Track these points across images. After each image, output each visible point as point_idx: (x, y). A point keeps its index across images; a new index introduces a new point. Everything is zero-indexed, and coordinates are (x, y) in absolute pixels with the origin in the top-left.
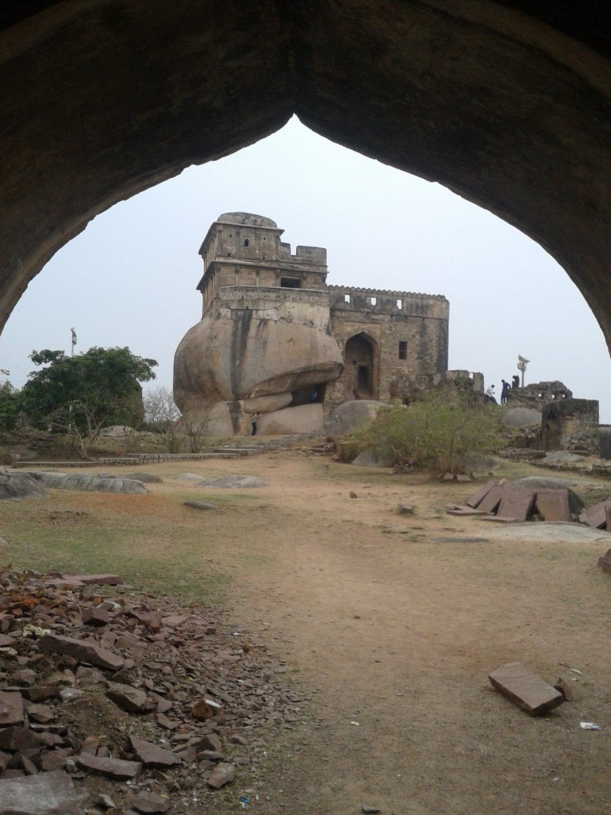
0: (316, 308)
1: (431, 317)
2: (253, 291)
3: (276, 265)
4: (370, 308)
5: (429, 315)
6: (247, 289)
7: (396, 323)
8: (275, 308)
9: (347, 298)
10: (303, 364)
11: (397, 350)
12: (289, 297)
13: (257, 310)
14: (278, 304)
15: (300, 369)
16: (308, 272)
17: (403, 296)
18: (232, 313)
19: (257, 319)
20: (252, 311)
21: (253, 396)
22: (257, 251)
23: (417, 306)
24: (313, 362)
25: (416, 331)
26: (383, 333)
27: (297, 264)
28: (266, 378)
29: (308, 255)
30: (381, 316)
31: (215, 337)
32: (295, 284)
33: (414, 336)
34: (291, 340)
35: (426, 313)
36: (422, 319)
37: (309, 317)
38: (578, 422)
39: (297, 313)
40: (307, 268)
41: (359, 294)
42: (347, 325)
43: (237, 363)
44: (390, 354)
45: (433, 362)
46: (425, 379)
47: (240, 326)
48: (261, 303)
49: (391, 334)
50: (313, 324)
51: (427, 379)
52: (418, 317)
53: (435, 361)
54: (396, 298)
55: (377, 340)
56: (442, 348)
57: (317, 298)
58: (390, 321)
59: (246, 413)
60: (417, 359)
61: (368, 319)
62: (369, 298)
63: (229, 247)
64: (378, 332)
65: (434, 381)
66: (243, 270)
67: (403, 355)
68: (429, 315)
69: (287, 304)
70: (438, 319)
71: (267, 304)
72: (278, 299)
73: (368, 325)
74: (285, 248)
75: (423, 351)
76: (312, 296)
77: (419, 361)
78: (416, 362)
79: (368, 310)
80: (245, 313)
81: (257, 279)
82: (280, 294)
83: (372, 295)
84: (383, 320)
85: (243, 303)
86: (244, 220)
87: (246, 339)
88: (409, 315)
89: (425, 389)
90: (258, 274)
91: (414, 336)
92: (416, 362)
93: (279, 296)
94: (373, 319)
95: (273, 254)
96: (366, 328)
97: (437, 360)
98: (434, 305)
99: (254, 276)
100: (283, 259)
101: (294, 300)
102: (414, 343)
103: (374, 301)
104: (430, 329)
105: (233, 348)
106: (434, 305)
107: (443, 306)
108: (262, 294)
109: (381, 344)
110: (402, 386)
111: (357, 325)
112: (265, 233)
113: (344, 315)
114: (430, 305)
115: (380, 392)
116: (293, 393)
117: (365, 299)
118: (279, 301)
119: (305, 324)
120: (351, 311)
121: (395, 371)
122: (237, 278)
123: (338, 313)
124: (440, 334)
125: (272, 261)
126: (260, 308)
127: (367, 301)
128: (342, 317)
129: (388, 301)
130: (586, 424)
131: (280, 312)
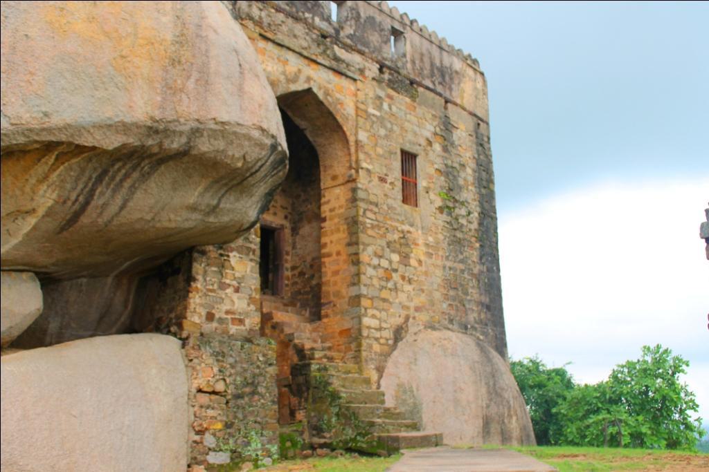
15: (125, 128)
24: (188, 110)
49: (381, 120)
58: (378, 81)
67: (409, 194)
84: (362, 71)
91: (430, 143)
94: (336, 59)
109: (357, 142)
111: (294, 63)
115: (365, 302)
116: (48, 281)
121: (396, 236)
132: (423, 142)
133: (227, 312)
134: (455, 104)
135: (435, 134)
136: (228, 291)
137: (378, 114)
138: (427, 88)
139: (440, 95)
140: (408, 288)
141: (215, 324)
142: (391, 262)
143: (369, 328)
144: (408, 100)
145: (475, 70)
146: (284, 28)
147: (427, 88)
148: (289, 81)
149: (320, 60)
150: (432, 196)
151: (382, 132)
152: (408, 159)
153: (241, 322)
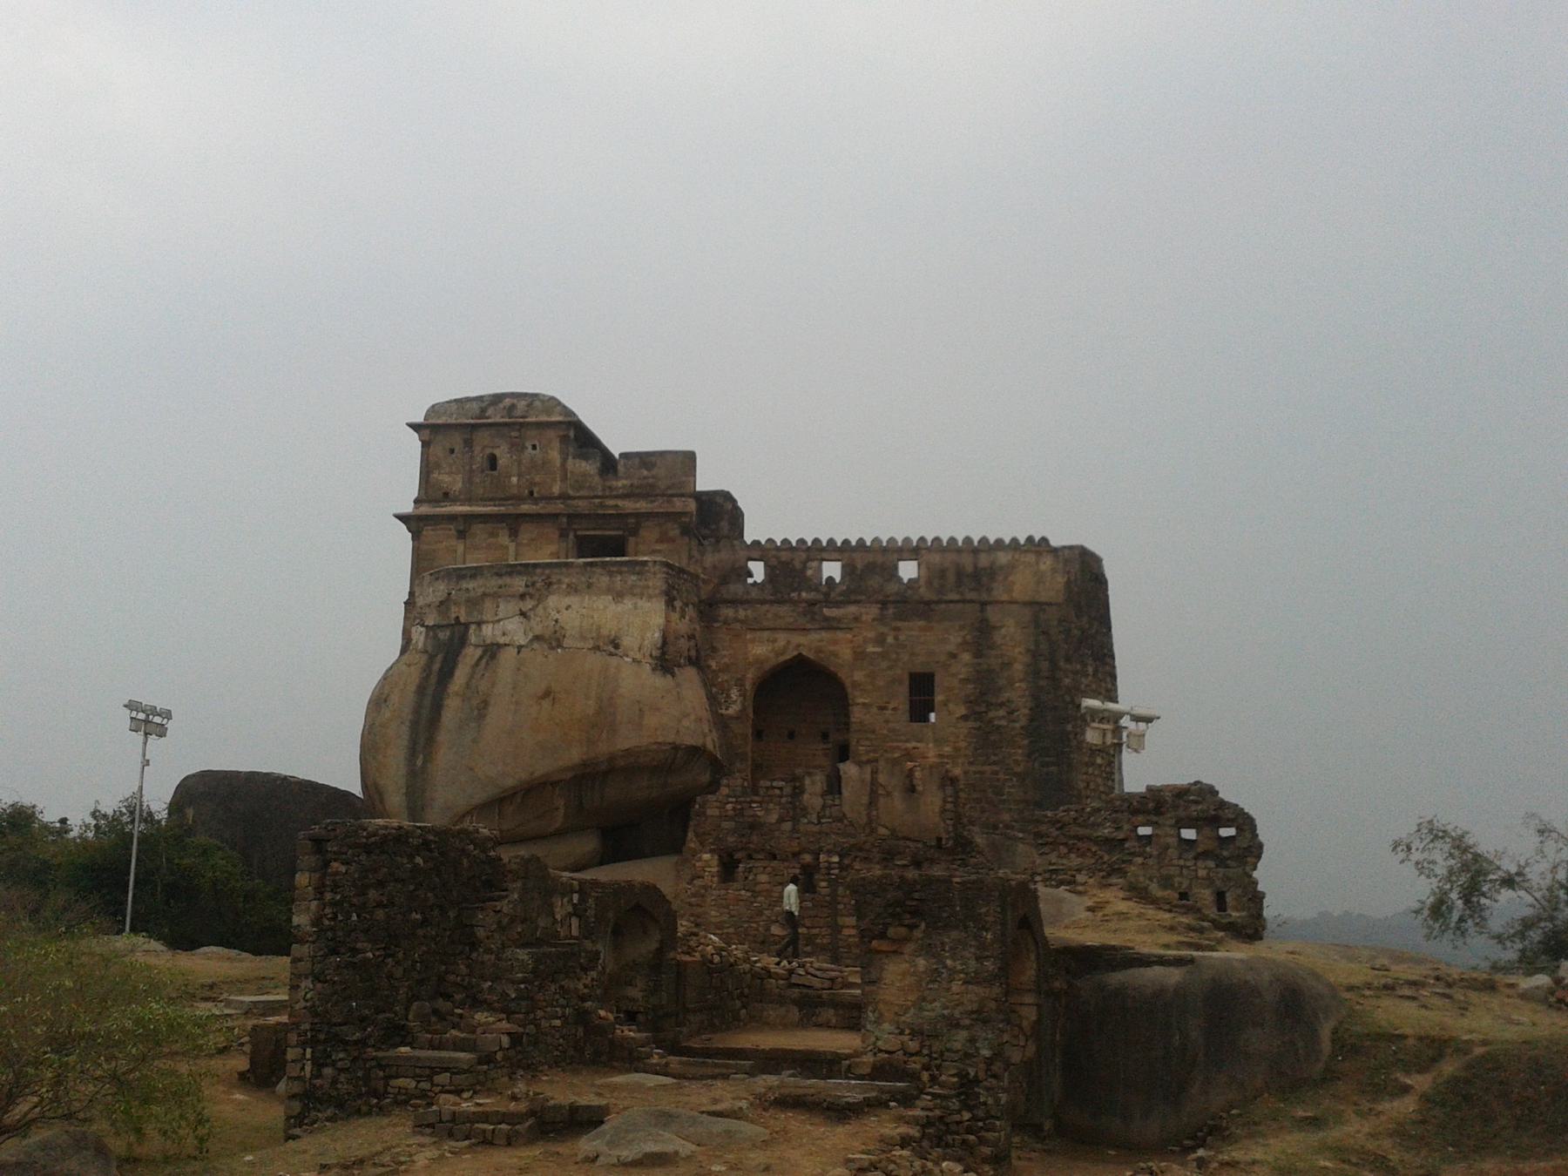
0: (628, 603)
1: (1005, 597)
2: (473, 577)
3: (559, 507)
4: (817, 590)
5: (999, 593)
6: (461, 575)
7: (895, 624)
8: (523, 614)
9: (758, 570)
10: (575, 755)
11: (901, 700)
12: (559, 582)
13: (479, 624)
14: (528, 604)
16: (638, 516)
17: (914, 550)
19: (477, 646)
20: (467, 626)
22: (514, 480)
23: (960, 574)
24: (603, 749)
25: (959, 640)
26: (860, 655)
27: (617, 497)
28: (480, 796)
29: (645, 473)
30: (852, 609)
32: (617, 547)
33: (953, 656)
34: (547, 694)
35: (989, 590)
36: (977, 607)
37: (610, 628)
38: (921, 963)
39: (577, 623)
40: (642, 506)
41: (784, 556)
42: (753, 641)
43: (419, 762)
44: (882, 708)
45: (1017, 725)
46: (781, 789)
47: (436, 666)
48: (488, 604)
49: (883, 655)
50: (617, 646)
51: (788, 790)
52: (964, 601)
53: (1023, 722)
54: (896, 556)
55: (842, 675)
56: (1042, 683)
57: (634, 578)
60: (965, 718)
61: (813, 619)
62: (815, 564)
63: (446, 478)
64: (846, 653)
65: (806, 796)
66: (478, 528)
68: (999, 593)
69: (552, 601)
70: (1025, 604)
71: (502, 607)
72: (531, 590)
73: (814, 636)
74: (584, 464)
75: (982, 694)
76: (621, 573)
77: (970, 724)
78: (964, 728)
79: (812, 596)
80: (453, 634)
81: (512, 547)
83: (825, 555)
85: (448, 609)
86: (483, 410)
87: (442, 699)
88: (935, 598)
89: (781, 820)
90: (514, 533)
92: (964, 728)
93: (533, 584)
94: (827, 619)
95: (554, 480)
96: (809, 643)
97: (1032, 720)
98: (1012, 567)
99: (504, 539)
100: (581, 488)
101: (573, 590)
102: (954, 675)
103: (832, 570)
104: (1003, 631)
105: (414, 724)
106: (1012, 567)
107: (1043, 567)
108: (493, 583)
110: (716, 812)
111: (782, 638)
112: (533, 433)
113: (742, 614)
114: (1001, 568)
117: (805, 567)
118: (531, 596)
119: (597, 648)
120: (763, 602)
122: (461, 548)
123: (727, 612)
124: (1037, 643)
125: (549, 499)
127: (809, 572)
128: (737, 620)
129: (871, 568)
130: (953, 971)
131: (533, 623)
135: (965, 643)
137: (878, 650)
144: (922, 623)
145: (1039, 554)
146: (770, 615)
148: (778, 655)
149: (809, 626)
150: (951, 706)
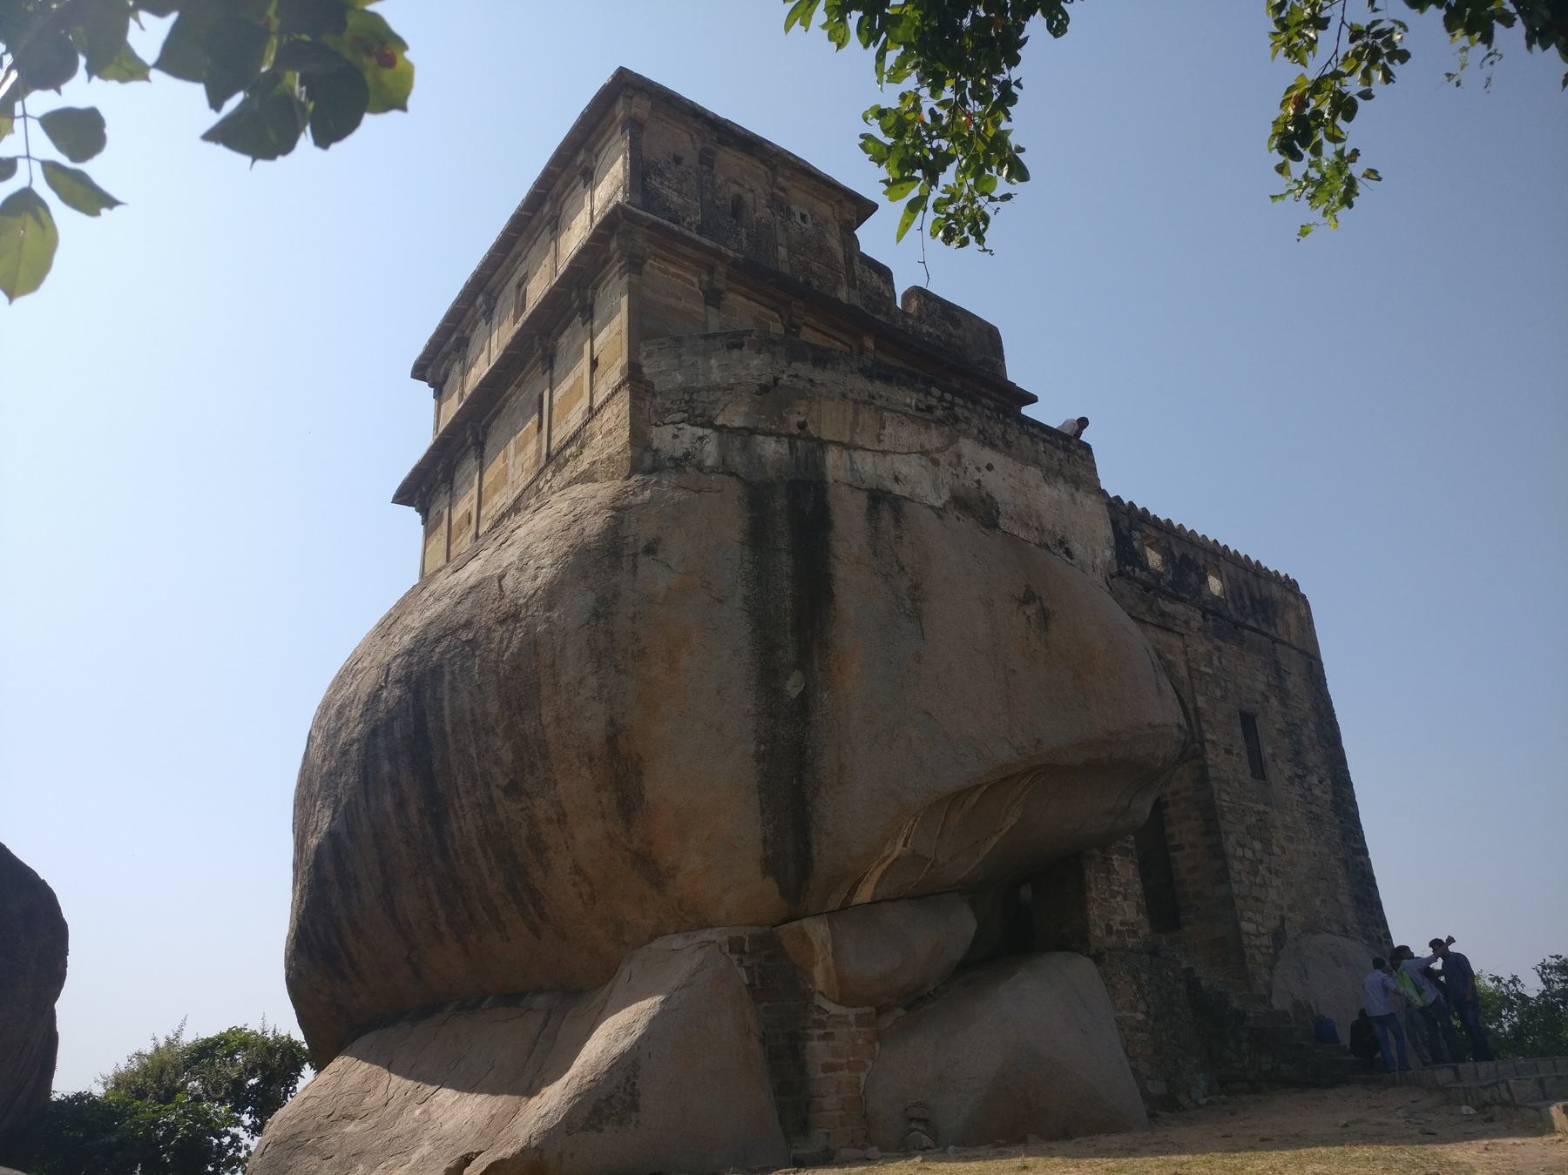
8: (924, 453)
18: (722, 445)
21: (865, 894)
31: (650, 550)
50: (1068, 552)
59: (843, 1001)
71: (889, 430)
74: (875, 277)
82: (934, 402)
84: (1187, 623)
91: (1266, 699)
94: (1163, 614)
115: (1239, 903)
126: (859, 441)
132: (1258, 698)
133: (1122, 924)
134: (1283, 643)
136: (1117, 902)
138: (1253, 630)
139: (1266, 635)
140: (1276, 882)
141: (1114, 938)
142: (1254, 851)
143: (1248, 934)
144: (1235, 648)
147: (1253, 630)
149: (1148, 619)
151: (1218, 693)
152: (1248, 721)
153: (1135, 933)
